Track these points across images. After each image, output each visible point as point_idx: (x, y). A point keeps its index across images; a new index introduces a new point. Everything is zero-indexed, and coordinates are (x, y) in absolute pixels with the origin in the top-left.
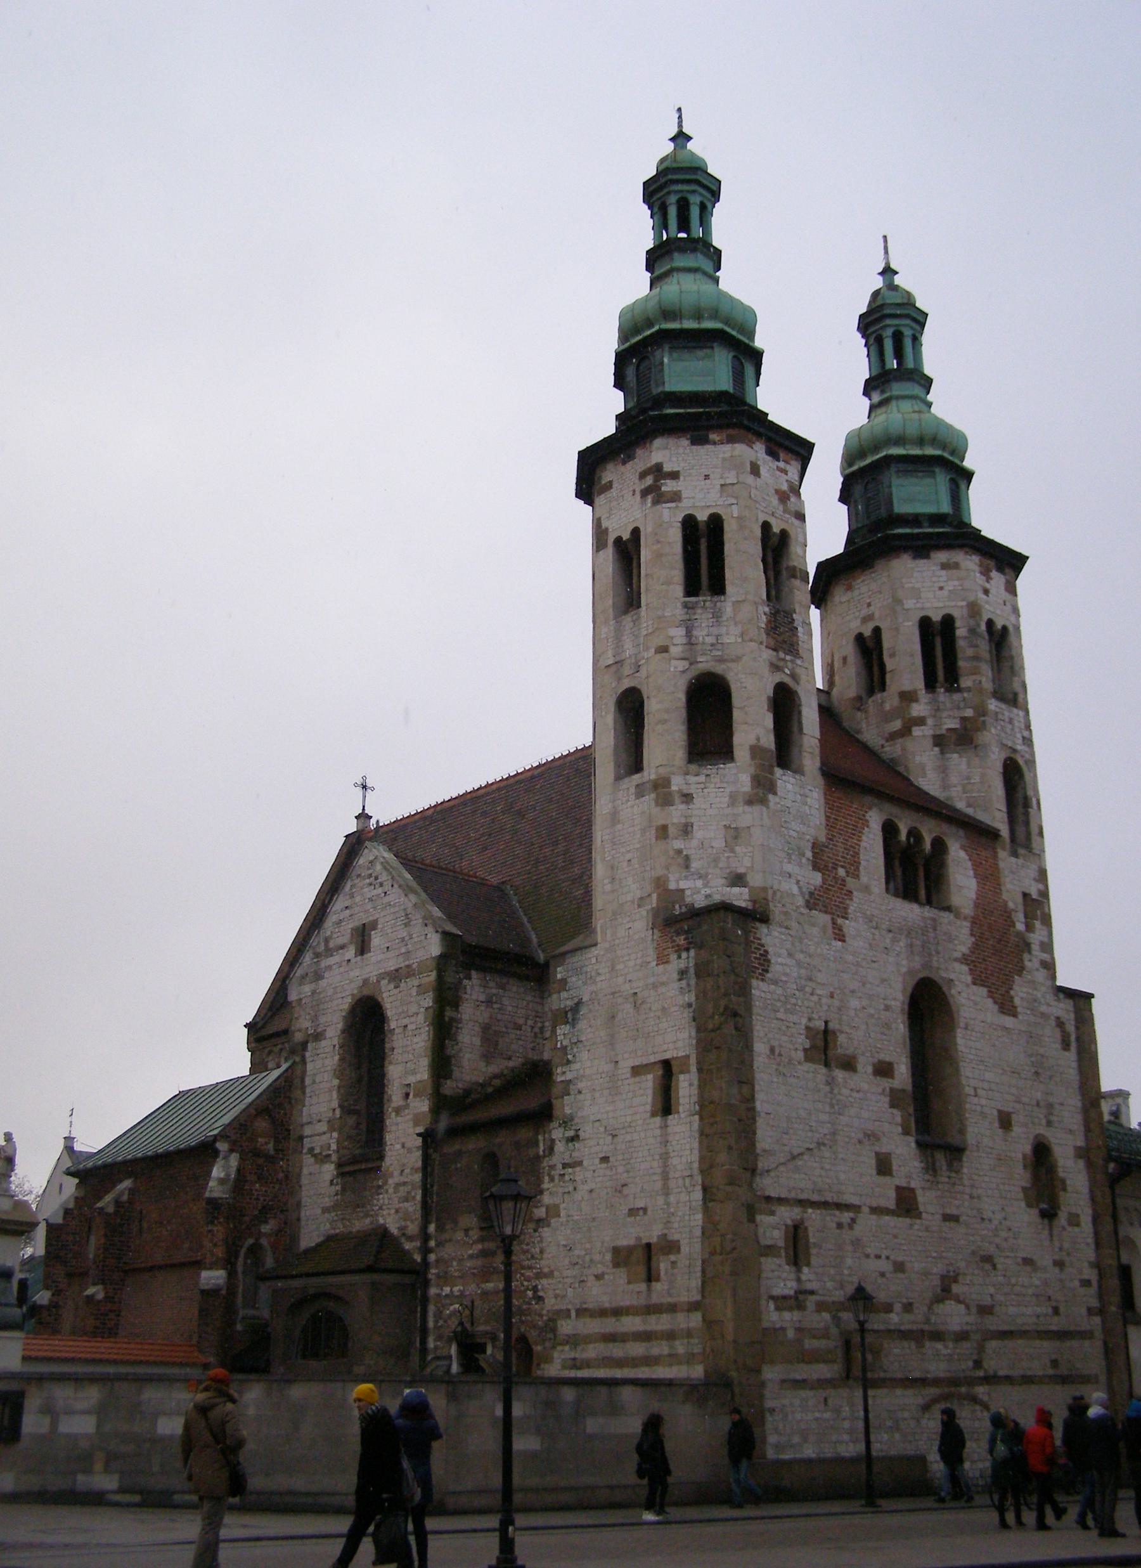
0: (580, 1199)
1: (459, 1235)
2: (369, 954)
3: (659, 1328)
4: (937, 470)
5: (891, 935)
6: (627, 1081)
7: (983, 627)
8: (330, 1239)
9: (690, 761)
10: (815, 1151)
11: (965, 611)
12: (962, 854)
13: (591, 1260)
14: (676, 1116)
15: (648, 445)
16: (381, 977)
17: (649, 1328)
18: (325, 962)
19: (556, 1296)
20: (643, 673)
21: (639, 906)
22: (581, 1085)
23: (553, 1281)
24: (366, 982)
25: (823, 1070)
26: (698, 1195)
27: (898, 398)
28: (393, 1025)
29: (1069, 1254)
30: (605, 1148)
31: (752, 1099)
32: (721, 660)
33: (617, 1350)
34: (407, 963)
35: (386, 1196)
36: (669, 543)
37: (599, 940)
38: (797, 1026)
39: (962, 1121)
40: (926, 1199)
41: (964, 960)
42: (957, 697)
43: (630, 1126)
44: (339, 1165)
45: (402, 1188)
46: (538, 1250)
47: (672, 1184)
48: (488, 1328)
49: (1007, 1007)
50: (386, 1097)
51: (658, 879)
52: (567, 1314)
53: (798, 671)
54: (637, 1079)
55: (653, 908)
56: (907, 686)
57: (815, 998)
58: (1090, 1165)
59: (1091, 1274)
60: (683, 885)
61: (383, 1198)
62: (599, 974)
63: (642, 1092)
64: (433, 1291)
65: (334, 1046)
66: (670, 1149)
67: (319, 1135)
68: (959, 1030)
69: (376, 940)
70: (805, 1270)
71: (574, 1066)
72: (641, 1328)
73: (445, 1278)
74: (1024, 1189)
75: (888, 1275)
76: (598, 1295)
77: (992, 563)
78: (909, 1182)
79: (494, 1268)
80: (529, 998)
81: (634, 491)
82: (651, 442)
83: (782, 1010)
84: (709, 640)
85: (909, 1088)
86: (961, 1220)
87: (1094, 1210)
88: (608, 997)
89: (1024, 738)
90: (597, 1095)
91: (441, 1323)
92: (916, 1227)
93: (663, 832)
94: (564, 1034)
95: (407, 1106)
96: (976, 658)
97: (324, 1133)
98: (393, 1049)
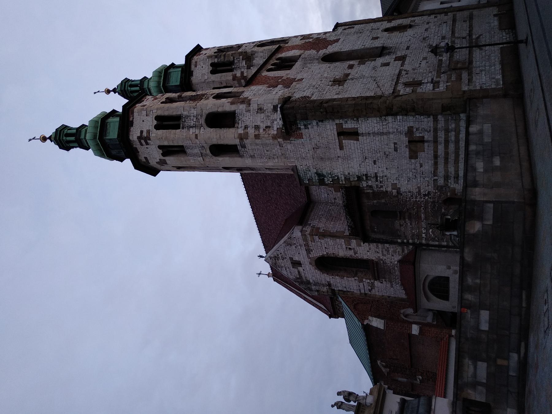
0: (390, 173)
1: (403, 229)
2: (301, 261)
3: (443, 136)
4: (169, 71)
5: (305, 68)
6: (345, 152)
7: (216, 54)
8: (402, 285)
9: (233, 126)
10: (377, 81)
11: (210, 59)
12: (283, 54)
13: (415, 169)
14: (359, 129)
15: (132, 142)
17: (443, 142)
19: (428, 186)
20: (205, 145)
21: (282, 147)
22: (347, 174)
23: (422, 186)
24: (310, 264)
25: (348, 81)
26: (390, 119)
27: (148, 86)
28: (325, 253)
29: (425, 21)
30: (370, 162)
31: (354, 98)
32: (202, 116)
33: (452, 157)
34: (304, 246)
35: (387, 260)
36: (162, 134)
37: (295, 164)
38: (330, 88)
39: (373, 48)
40: (399, 54)
41: (318, 52)
42: (236, 62)
43: (362, 150)
44: (375, 279)
45: (384, 253)
46: (409, 194)
47: (385, 131)
48: (440, 217)
49: (337, 41)
50: (350, 258)
51: (273, 138)
52: (435, 181)
53: (210, 94)
54: (345, 147)
55: (283, 140)
56: (231, 78)
57: (321, 84)
58: (393, 20)
59: (433, 16)
60: (275, 129)
61: (388, 261)
62: (306, 165)
63: (349, 145)
64: (424, 242)
65: (333, 278)
66: (371, 131)
67: (364, 286)
68: (341, 51)
69: (296, 258)
70: (423, 81)
71: (340, 176)
72: (443, 145)
73: (419, 236)
74: (399, 33)
75: (428, 61)
76: (428, 167)
77: (198, 53)
78: (393, 58)
79: (416, 214)
80: (320, 207)
81: (147, 148)
82: (131, 140)
83: (323, 92)
84: (195, 120)
85: (359, 60)
86: (408, 45)
87: (410, 17)
88: (315, 161)
89: (252, 43)
90: (350, 166)
91: (436, 239)
92: (410, 55)
94: (328, 180)
95: (354, 249)
96: (225, 56)
97: (363, 284)
98: (333, 253)
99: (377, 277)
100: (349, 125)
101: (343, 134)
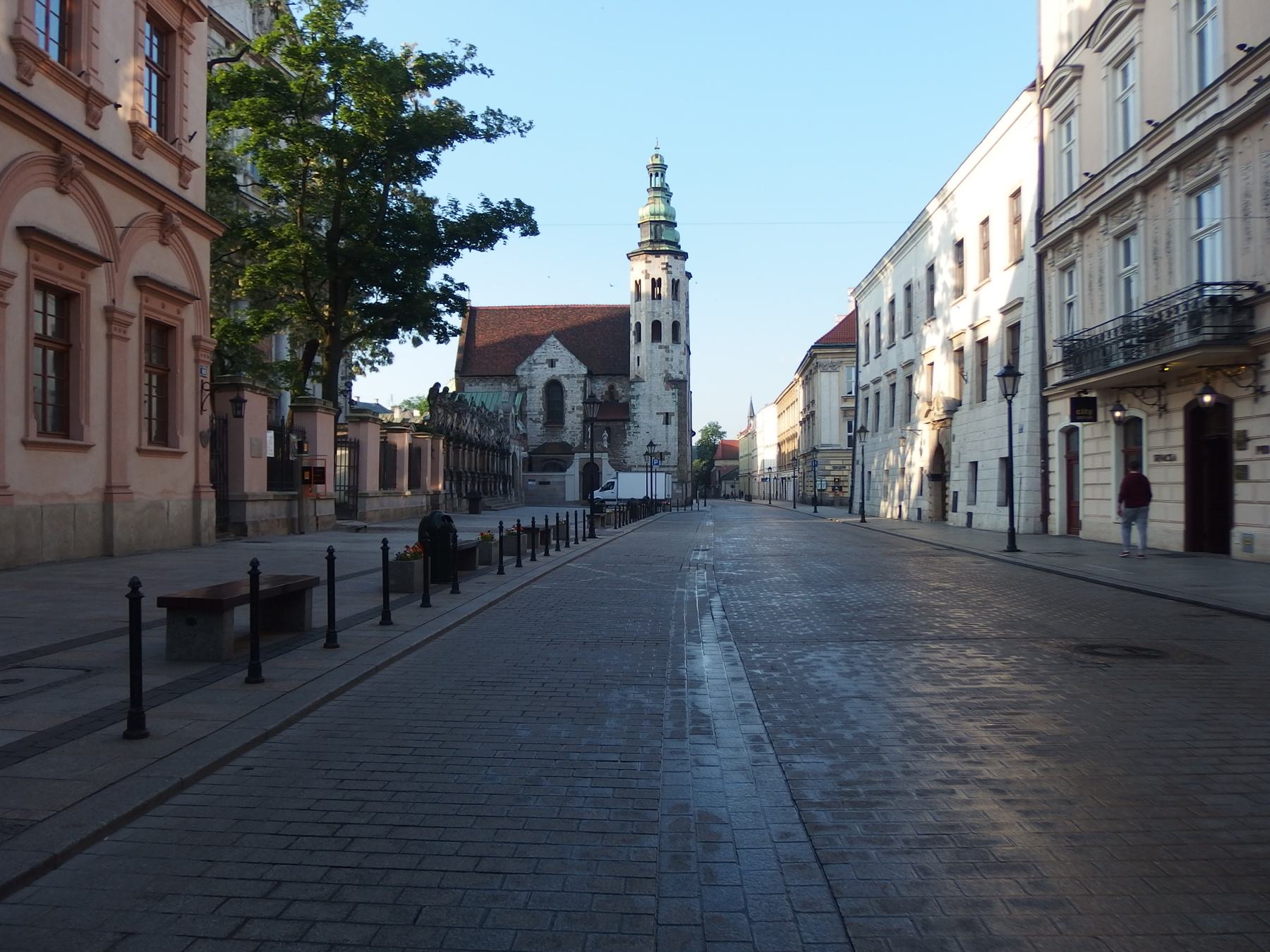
16: (560, 376)
18: (533, 367)
20: (662, 317)
93: (667, 359)
99: (545, 425)
100: (674, 420)
101: (667, 417)
